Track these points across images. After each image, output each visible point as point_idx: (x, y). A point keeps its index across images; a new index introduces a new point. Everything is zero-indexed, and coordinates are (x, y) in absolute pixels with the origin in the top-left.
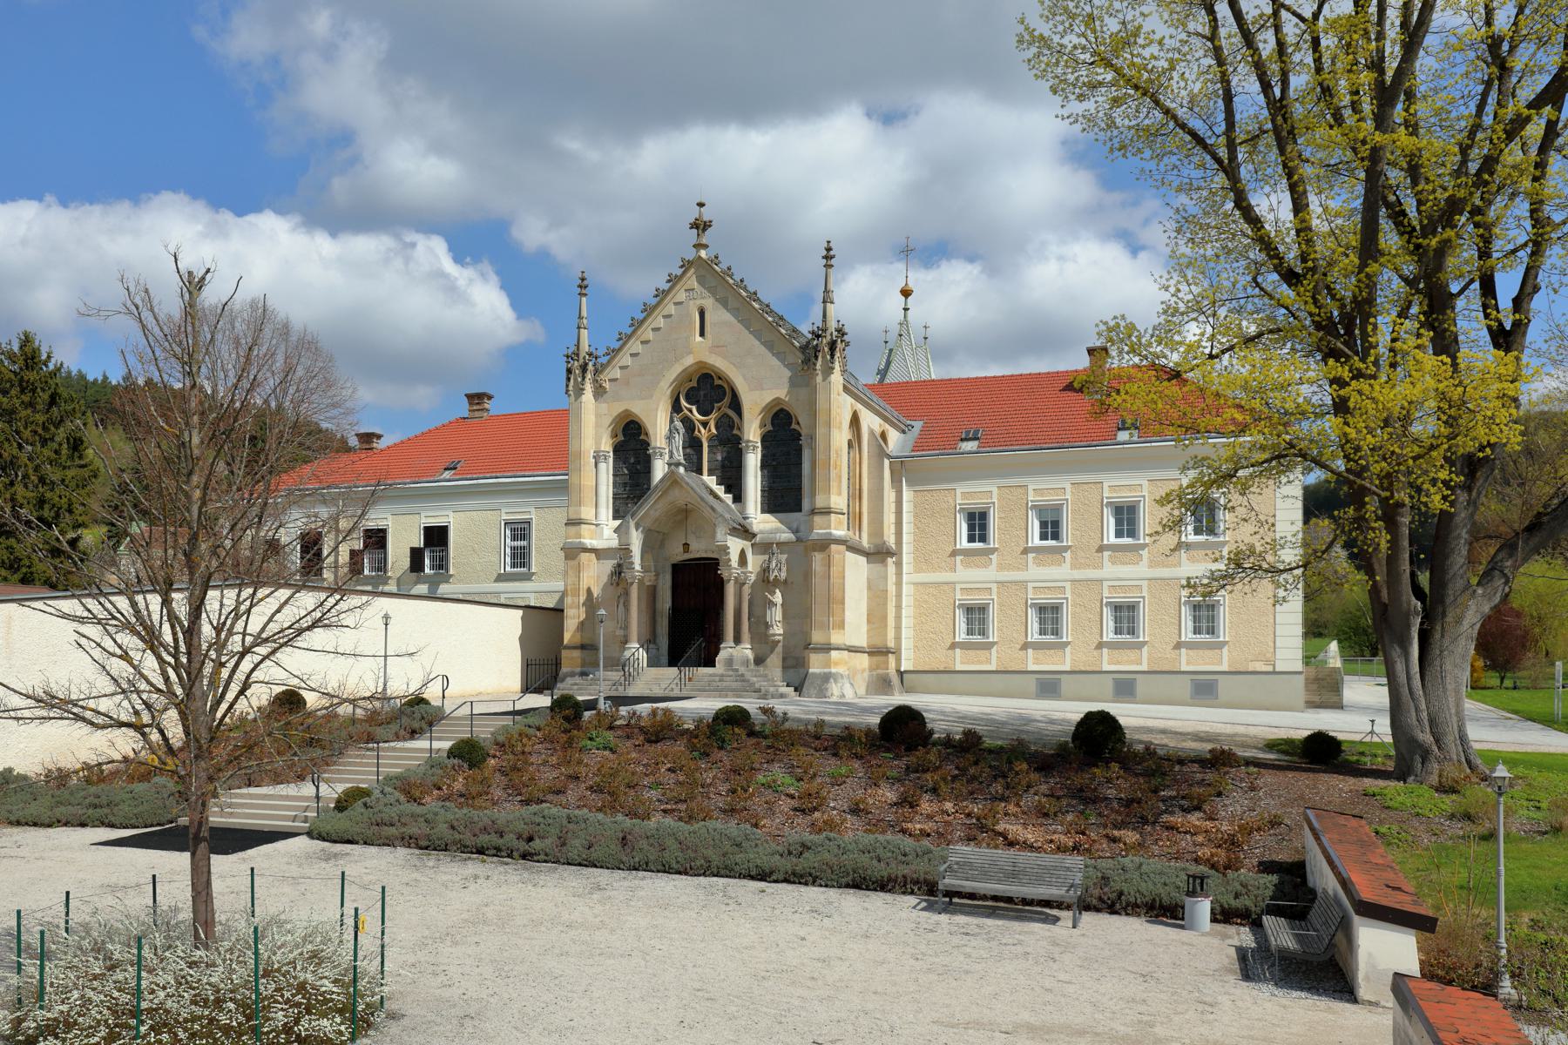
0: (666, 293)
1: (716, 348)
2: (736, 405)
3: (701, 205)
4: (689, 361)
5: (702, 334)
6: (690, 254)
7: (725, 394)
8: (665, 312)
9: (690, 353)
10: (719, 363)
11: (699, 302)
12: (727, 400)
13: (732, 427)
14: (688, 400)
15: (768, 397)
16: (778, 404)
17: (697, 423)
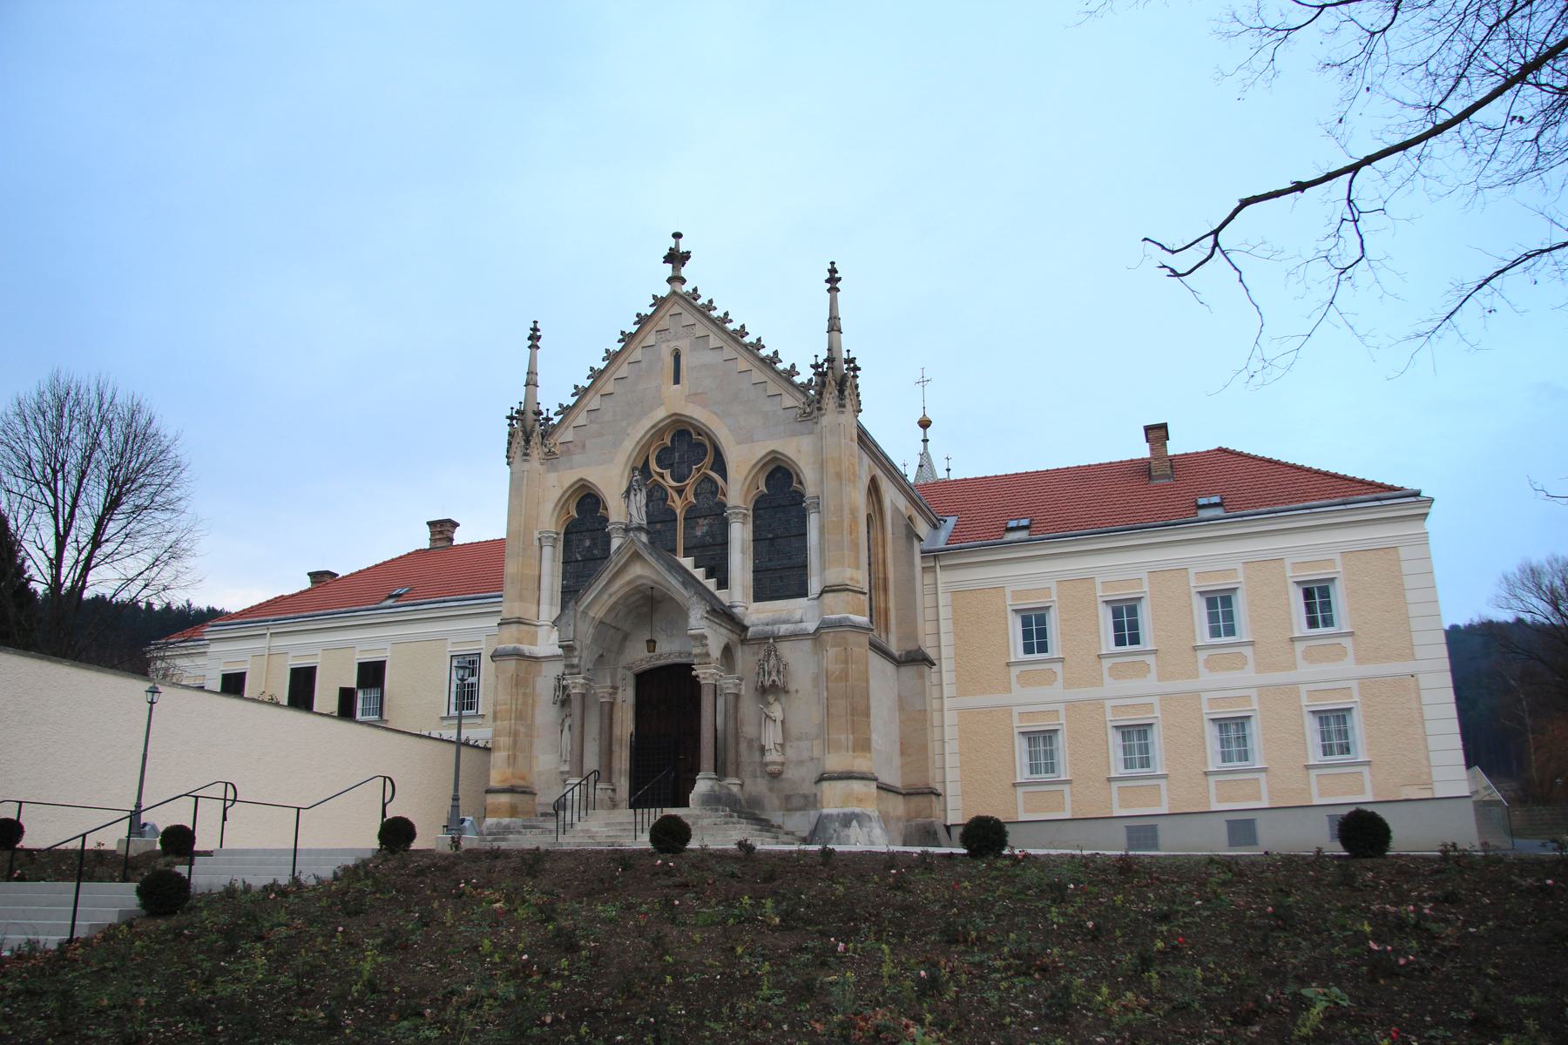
0: (632, 336)
1: (693, 397)
2: (720, 465)
3: (677, 236)
4: (660, 414)
5: (677, 381)
6: (664, 290)
7: (705, 455)
8: (632, 359)
9: (662, 404)
10: (698, 413)
11: (673, 344)
12: (709, 459)
13: (715, 493)
14: (659, 462)
15: (760, 450)
16: (775, 459)
17: (670, 490)
